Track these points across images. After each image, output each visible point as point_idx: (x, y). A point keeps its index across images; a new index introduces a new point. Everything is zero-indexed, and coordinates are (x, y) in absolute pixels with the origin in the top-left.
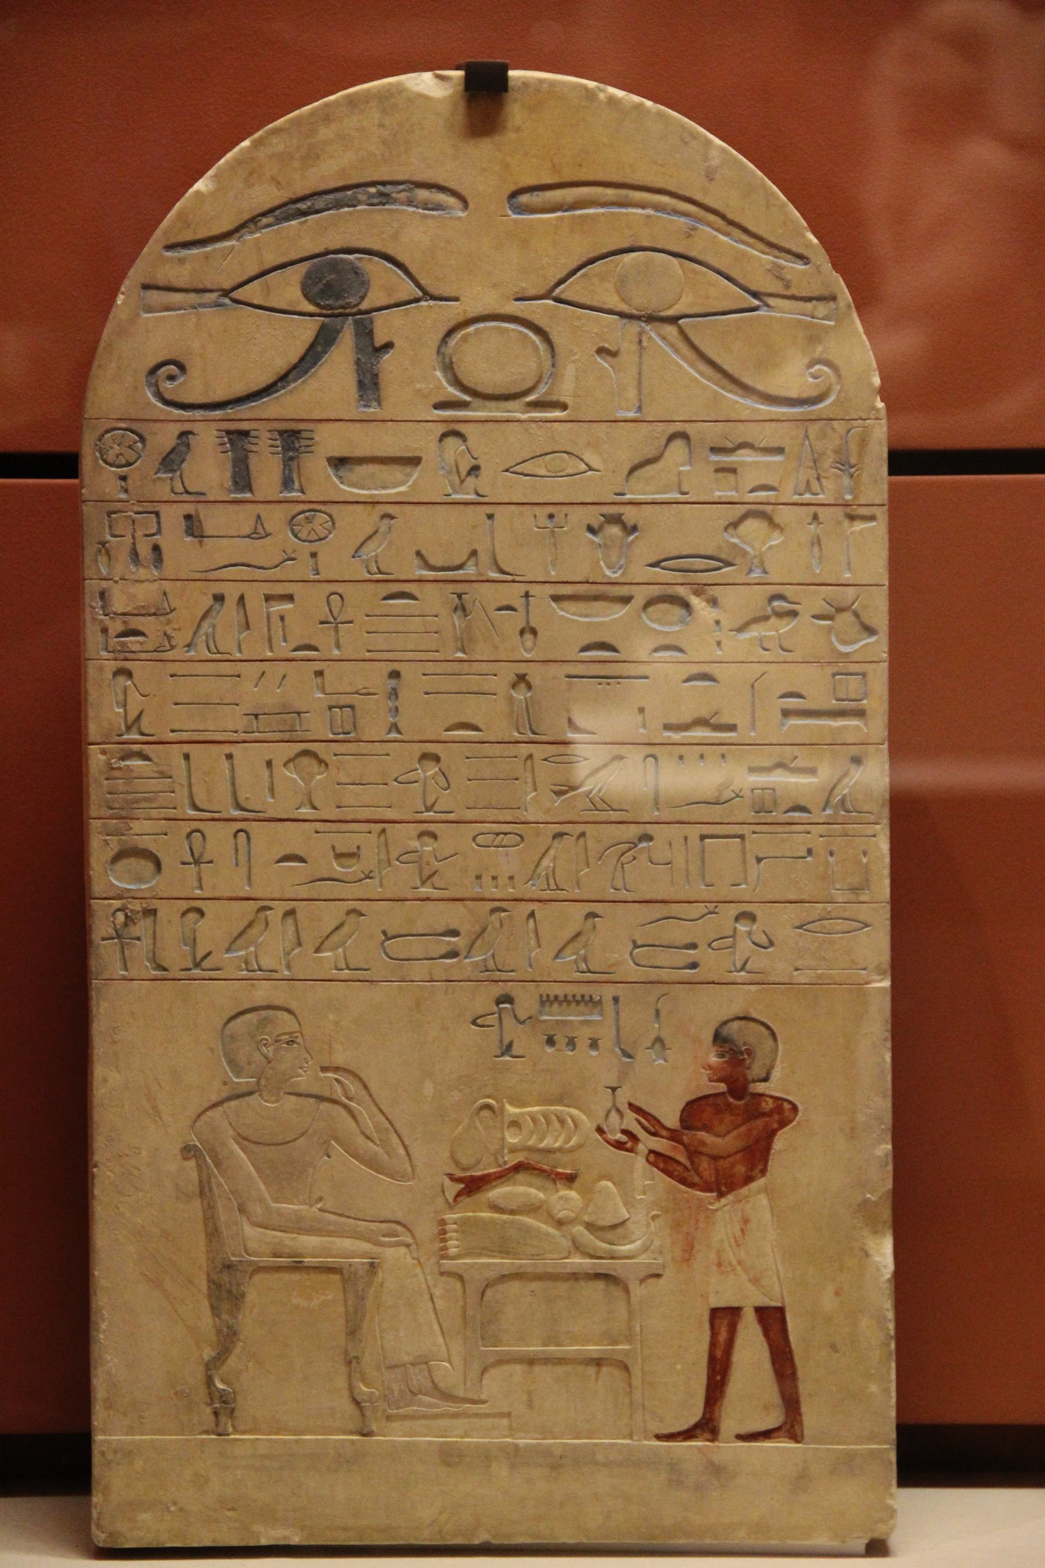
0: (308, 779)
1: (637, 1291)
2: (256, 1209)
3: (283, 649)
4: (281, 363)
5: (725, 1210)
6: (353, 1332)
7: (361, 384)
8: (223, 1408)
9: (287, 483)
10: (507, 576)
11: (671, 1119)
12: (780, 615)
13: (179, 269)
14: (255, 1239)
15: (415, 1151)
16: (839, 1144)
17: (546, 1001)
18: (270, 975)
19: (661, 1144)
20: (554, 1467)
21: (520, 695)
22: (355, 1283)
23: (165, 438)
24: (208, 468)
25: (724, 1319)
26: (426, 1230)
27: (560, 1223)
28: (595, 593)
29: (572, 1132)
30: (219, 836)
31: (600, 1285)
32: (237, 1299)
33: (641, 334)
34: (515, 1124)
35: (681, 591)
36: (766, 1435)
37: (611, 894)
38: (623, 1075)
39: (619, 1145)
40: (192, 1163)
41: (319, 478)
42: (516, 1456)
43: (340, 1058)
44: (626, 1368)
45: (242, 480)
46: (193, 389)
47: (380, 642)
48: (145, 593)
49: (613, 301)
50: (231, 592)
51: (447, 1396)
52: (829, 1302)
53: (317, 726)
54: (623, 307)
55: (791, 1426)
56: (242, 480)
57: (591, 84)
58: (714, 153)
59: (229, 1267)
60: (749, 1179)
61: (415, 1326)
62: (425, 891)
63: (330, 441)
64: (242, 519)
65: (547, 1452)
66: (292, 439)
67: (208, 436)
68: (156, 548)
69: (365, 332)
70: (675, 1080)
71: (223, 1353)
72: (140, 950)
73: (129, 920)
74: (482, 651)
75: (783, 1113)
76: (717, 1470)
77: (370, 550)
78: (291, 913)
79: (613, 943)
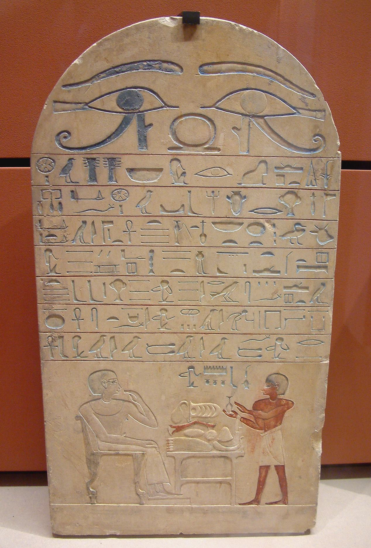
1: (235, 461)
2: (103, 436)
3: (109, 241)
4: (108, 132)
6: (137, 474)
7: (139, 139)
8: (93, 497)
9: (111, 178)
11: (250, 407)
14: (102, 446)
15: (158, 418)
17: (206, 368)
21: (199, 259)
22: (138, 460)
23: (63, 161)
24: (80, 172)
25: (264, 469)
26: (162, 443)
27: (209, 440)
29: (215, 411)
30: (86, 311)
31: (223, 459)
32: (97, 464)
33: (249, 122)
34: (194, 409)
36: (276, 503)
39: (231, 416)
41: (122, 172)
42: (192, 511)
43: (131, 387)
45: (93, 177)
49: (239, 109)
50: (89, 220)
52: (300, 463)
53: (122, 270)
56: (93, 177)
57: (233, 23)
59: (93, 454)
60: (275, 426)
61: (158, 470)
63: (127, 162)
64: (93, 192)
65: (203, 509)
66: (113, 161)
67: (79, 160)
68: (60, 203)
71: (92, 481)
74: (185, 243)
75: (289, 405)
77: (143, 204)
78: (113, 337)
79: (231, 348)
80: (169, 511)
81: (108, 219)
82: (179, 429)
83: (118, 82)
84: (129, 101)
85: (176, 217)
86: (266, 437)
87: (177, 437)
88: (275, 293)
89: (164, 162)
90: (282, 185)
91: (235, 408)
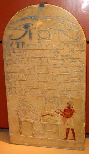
0: (26, 77)
1: (59, 126)
2: (23, 116)
3: (23, 64)
4: (22, 35)
5: (68, 120)
6: (32, 128)
7: (30, 37)
8: (21, 133)
9: (23, 47)
10: (45, 57)
11: (63, 111)
12: (74, 61)
13: (11, 26)
14: (23, 119)
15: (38, 112)
16: (80, 114)
17: (50, 99)
18: (23, 95)
19: (62, 113)
20: (52, 141)
21: (47, 69)
22: (33, 124)
23: (10, 43)
24: (15, 46)
25: (68, 130)
26: (39, 119)
27: (52, 120)
28: (54, 59)
29: (53, 111)
30: (17, 82)
31: (56, 125)
32: (21, 124)
33: (59, 32)
34: (47, 110)
35: (64, 59)
36: (72, 140)
37: (57, 89)
38: (58, 106)
39: (58, 113)
40: (17, 112)
41: (26, 46)
42: (48, 140)
43: (30, 103)
44: (58, 133)
45: (18, 47)
46: (13, 38)
47: (32, 63)
48: (9, 58)
49: (56, 28)
50: (17, 58)
51: (41, 134)
52: (78, 129)
53: (26, 71)
54: (57, 29)
55: (74, 139)
56: (18, 47)
57: (53, 5)
58: (66, 12)
59: (20, 121)
60: (70, 117)
61: (38, 128)
62: (38, 88)
63: (27, 43)
64: (18, 51)
65: (51, 139)
66: (23, 43)
67: (15, 43)
68: (10, 54)
69: (30, 31)
70: (63, 107)
71: (20, 129)
72: (11, 92)
73: (10, 89)
74: (43, 64)
75: (74, 111)
76: (67, 143)
77: (31, 54)
78: (25, 89)
79: (57, 94)
80: (42, 139)
81: (22, 58)
82: (43, 116)
83: (24, 22)
84: (26, 27)
85: (40, 58)
86: (68, 120)
87: (43, 118)
88: (68, 79)
89: (36, 43)
90: (69, 49)
91: (59, 111)
